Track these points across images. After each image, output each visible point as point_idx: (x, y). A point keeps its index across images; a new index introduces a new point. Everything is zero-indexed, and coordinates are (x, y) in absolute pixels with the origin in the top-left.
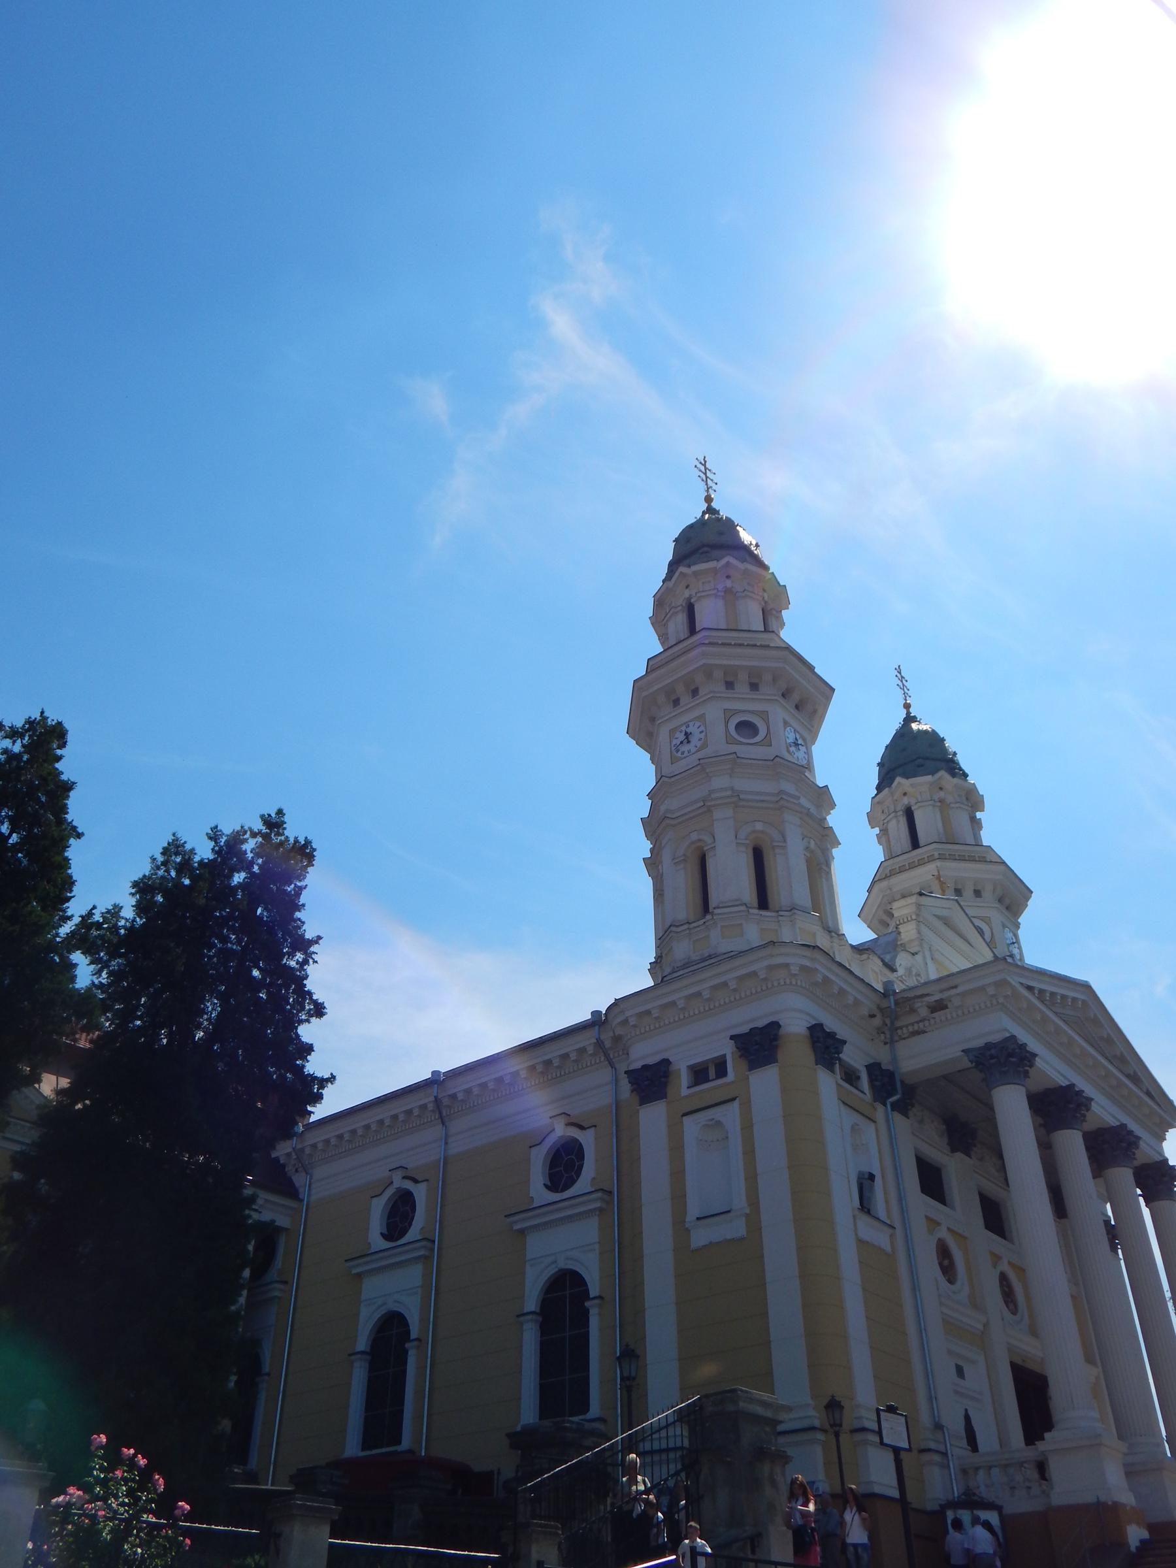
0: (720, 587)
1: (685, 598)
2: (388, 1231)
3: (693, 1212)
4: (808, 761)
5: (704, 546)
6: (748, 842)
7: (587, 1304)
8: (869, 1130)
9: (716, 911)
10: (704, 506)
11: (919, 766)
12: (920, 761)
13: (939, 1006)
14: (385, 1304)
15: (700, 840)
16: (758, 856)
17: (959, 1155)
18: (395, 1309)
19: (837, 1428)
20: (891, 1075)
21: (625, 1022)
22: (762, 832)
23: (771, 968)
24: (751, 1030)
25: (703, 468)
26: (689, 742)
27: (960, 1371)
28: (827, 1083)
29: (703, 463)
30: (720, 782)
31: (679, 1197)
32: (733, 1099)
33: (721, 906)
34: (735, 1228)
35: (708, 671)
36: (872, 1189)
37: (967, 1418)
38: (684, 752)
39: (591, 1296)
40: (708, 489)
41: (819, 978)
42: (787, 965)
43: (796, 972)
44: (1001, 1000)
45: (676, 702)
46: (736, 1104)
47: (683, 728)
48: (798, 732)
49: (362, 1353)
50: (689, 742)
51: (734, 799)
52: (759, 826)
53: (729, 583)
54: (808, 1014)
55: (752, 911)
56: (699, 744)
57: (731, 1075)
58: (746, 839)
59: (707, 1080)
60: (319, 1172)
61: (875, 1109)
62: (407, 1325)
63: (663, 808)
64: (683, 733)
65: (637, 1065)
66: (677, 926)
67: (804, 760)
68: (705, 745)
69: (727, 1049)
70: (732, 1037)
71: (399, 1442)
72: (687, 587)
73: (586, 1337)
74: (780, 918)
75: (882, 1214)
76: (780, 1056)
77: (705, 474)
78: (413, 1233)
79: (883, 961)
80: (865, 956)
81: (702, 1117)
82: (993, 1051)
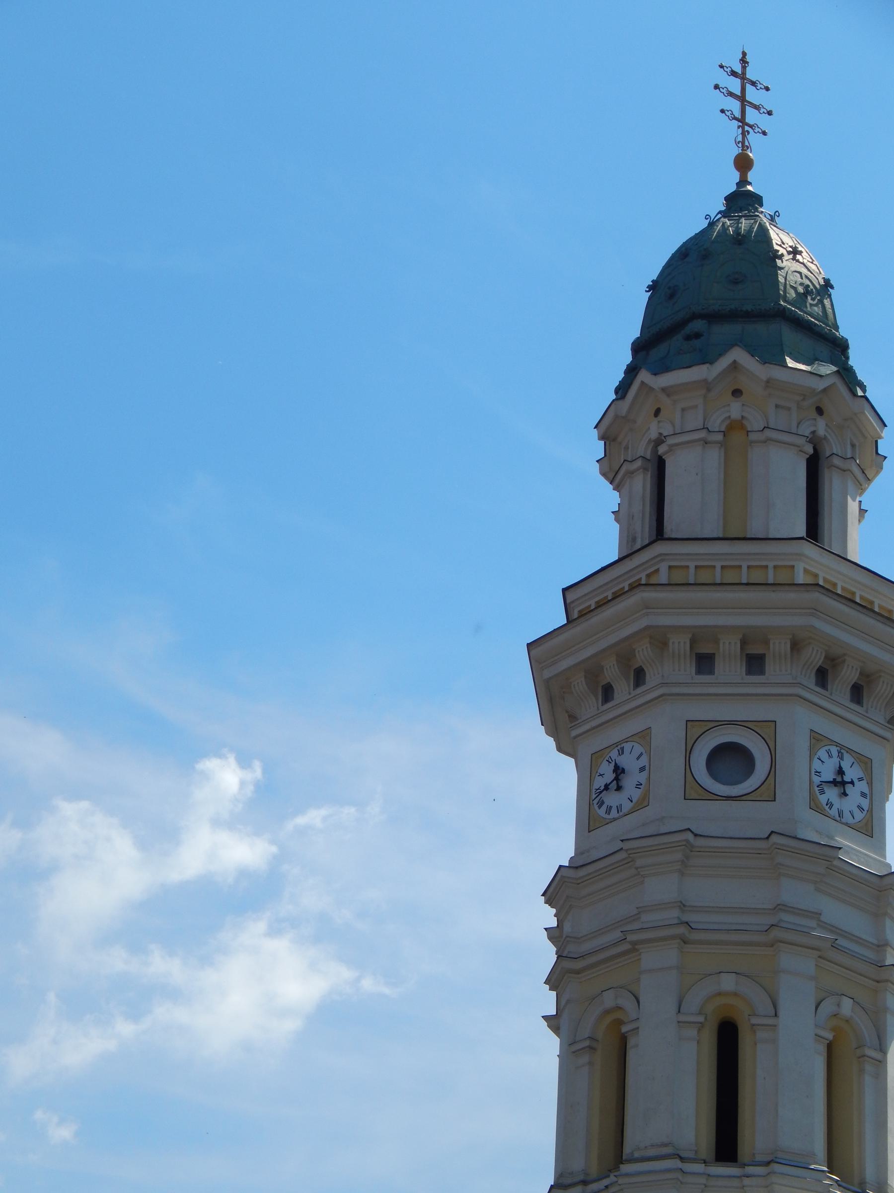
0: (717, 422)
1: (650, 440)
4: (870, 811)
5: (694, 317)
6: (701, 1019)
9: (625, 1168)
10: (729, 182)
15: (619, 1008)
25: (735, 85)
26: (619, 788)
29: (738, 69)
33: (637, 1155)
38: (611, 807)
40: (744, 134)
45: (608, 693)
47: (614, 754)
48: (850, 751)
50: (619, 788)
52: (728, 983)
53: (735, 410)
56: (636, 794)
58: (700, 1013)
63: (567, 928)
64: (612, 765)
68: (642, 804)
72: (657, 412)
74: (746, 1181)
77: (742, 99)
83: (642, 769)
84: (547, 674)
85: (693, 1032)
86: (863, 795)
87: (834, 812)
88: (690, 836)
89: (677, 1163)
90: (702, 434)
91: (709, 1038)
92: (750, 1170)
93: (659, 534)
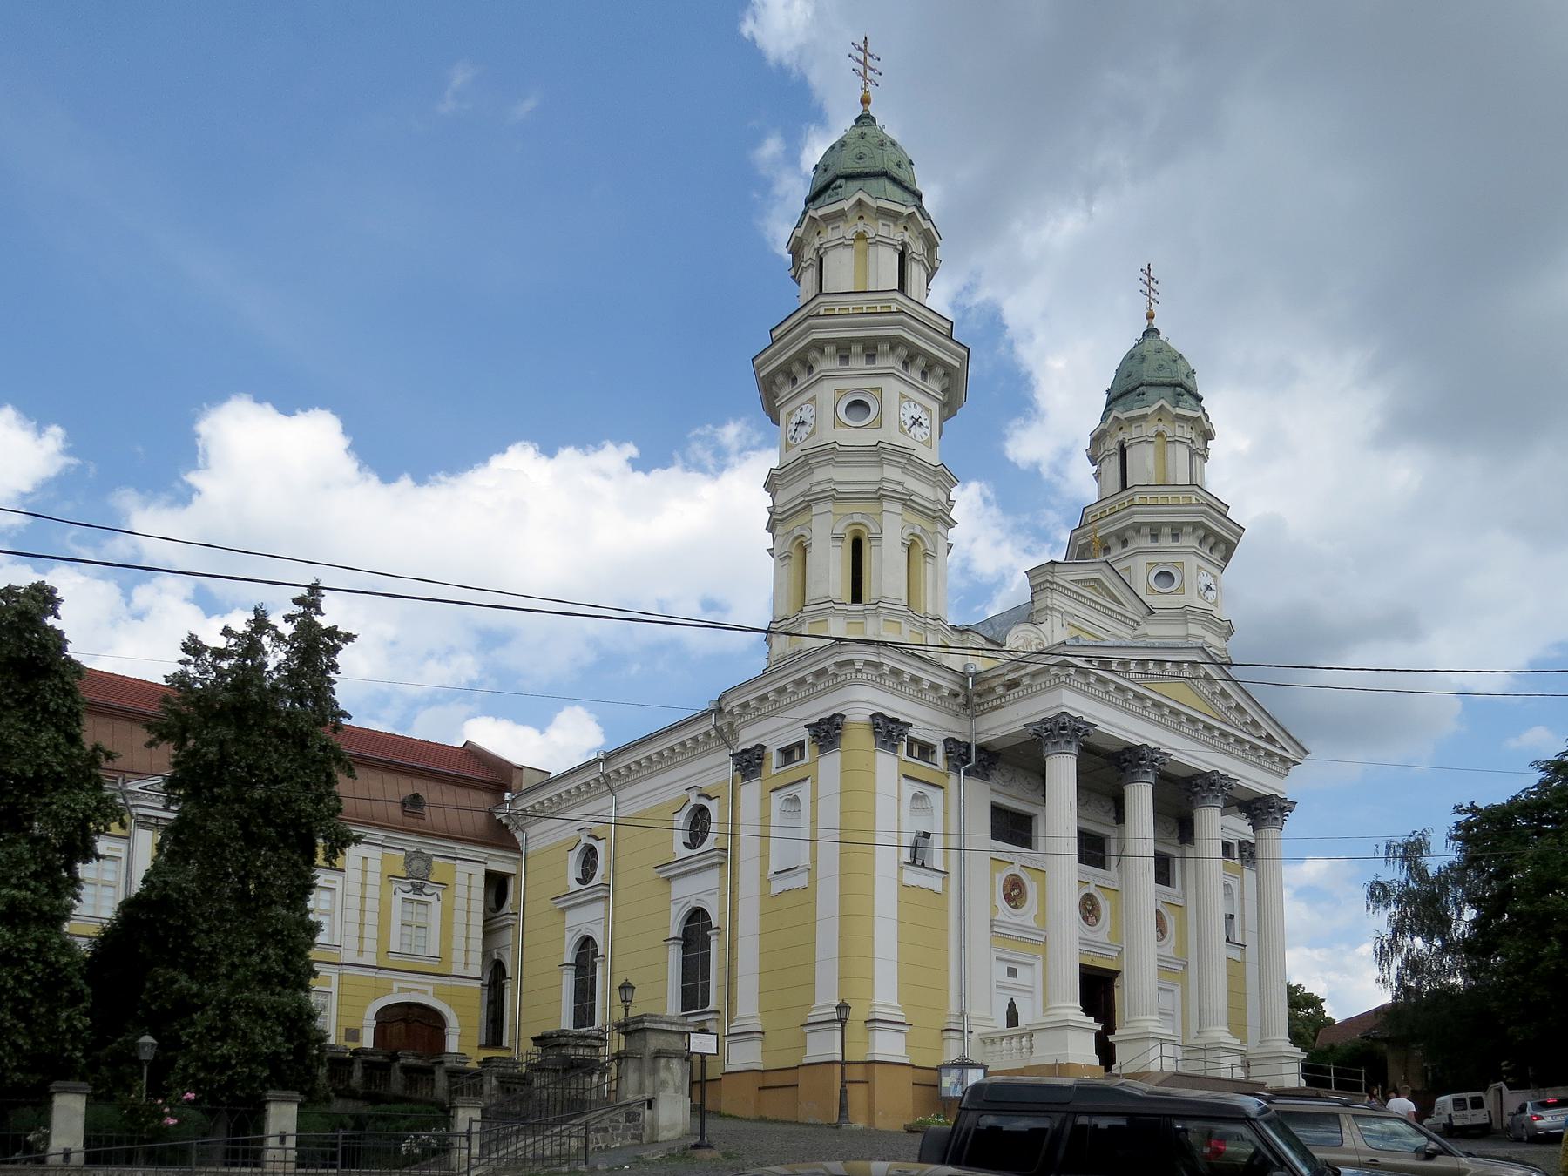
3: (771, 871)
8: (936, 797)
13: (1013, 685)
16: (857, 546)
20: (968, 746)
22: (861, 524)
23: (840, 665)
28: (887, 765)
32: (806, 779)
41: (886, 670)
42: (851, 663)
43: (861, 668)
46: (809, 781)
52: (857, 518)
61: (948, 777)
67: (924, 435)
69: (805, 735)
70: (806, 726)
74: (866, 612)
76: (843, 742)
80: (965, 637)
85: (840, 544)
86: (927, 427)
87: (912, 434)
88: (837, 446)
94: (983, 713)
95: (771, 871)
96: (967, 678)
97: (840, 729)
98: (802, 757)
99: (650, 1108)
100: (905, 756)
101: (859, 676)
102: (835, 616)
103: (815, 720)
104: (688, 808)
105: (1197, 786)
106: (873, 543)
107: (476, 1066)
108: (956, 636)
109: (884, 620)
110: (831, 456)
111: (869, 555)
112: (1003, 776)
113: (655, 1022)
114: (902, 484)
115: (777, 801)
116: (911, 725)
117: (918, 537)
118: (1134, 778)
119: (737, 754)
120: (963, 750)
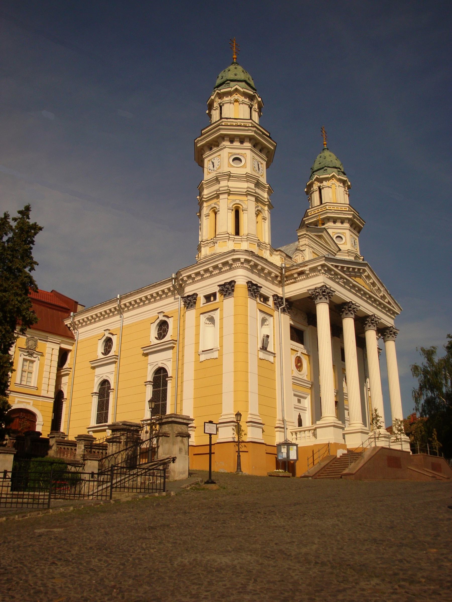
2: (104, 351)
4: (263, 173)
5: (228, 80)
7: (167, 379)
9: (217, 236)
11: (325, 170)
12: (326, 168)
14: (102, 377)
15: (215, 207)
17: (311, 326)
18: (106, 379)
19: (239, 422)
20: (282, 298)
21: (182, 280)
22: (239, 204)
23: (235, 260)
24: (225, 283)
27: (299, 401)
30: (223, 183)
31: (197, 343)
32: (217, 309)
33: (220, 234)
34: (215, 355)
35: (223, 137)
36: (267, 340)
37: (300, 416)
39: (169, 376)
42: (238, 260)
43: (243, 261)
44: (323, 271)
49: (96, 393)
51: (228, 191)
52: (238, 202)
54: (248, 277)
55: (230, 236)
56: (218, 167)
57: (218, 300)
59: (210, 301)
60: (80, 330)
61: (274, 311)
62: (110, 384)
65: (186, 295)
66: (203, 242)
69: (217, 289)
70: (218, 286)
71: (107, 422)
73: (166, 389)
74: (242, 239)
75: (272, 351)
78: (111, 354)
79: (286, 254)
80: (278, 253)
81: (207, 315)
82: (317, 290)
83: (219, 162)
84: (198, 145)
85: (231, 211)
87: (257, 172)
89: (228, 235)
90: (230, 101)
91: (234, 212)
92: (243, 237)
93: (221, 118)
94: (288, 284)
95: (201, 349)
96: (282, 269)
97: (234, 287)
98: (215, 299)
99: (173, 462)
100: (258, 301)
101: (242, 265)
102: (229, 239)
103: (223, 283)
104: (158, 321)
105: (367, 321)
106: (244, 212)
107: (74, 440)
108: (275, 253)
109: (250, 243)
110: (228, 177)
111: (244, 217)
112: (293, 312)
113: (177, 418)
114: (255, 190)
115: (203, 318)
116: (261, 287)
117: (260, 211)
118: (347, 315)
119: (185, 297)
120: (280, 300)
